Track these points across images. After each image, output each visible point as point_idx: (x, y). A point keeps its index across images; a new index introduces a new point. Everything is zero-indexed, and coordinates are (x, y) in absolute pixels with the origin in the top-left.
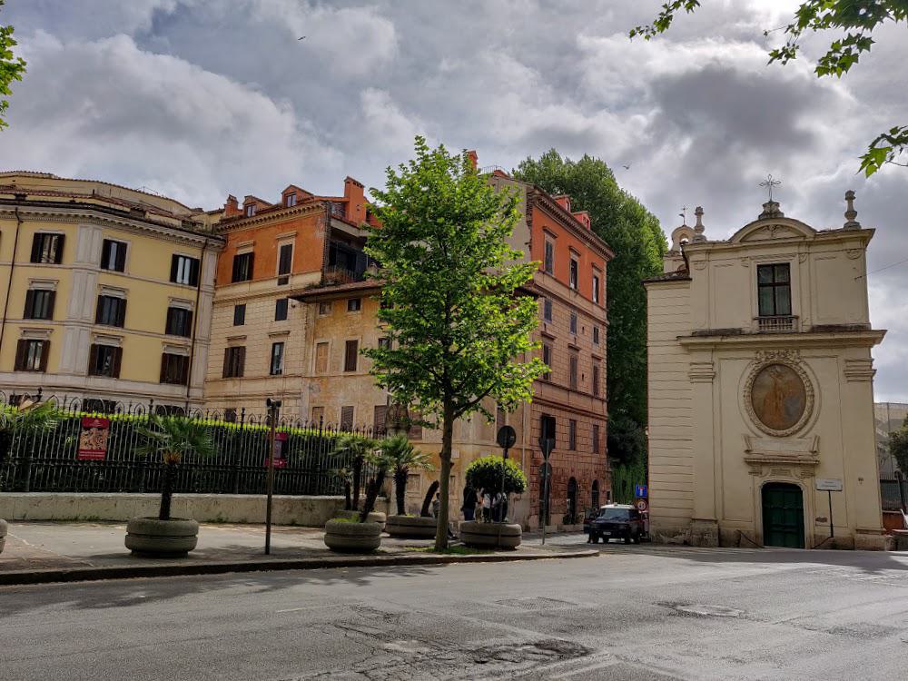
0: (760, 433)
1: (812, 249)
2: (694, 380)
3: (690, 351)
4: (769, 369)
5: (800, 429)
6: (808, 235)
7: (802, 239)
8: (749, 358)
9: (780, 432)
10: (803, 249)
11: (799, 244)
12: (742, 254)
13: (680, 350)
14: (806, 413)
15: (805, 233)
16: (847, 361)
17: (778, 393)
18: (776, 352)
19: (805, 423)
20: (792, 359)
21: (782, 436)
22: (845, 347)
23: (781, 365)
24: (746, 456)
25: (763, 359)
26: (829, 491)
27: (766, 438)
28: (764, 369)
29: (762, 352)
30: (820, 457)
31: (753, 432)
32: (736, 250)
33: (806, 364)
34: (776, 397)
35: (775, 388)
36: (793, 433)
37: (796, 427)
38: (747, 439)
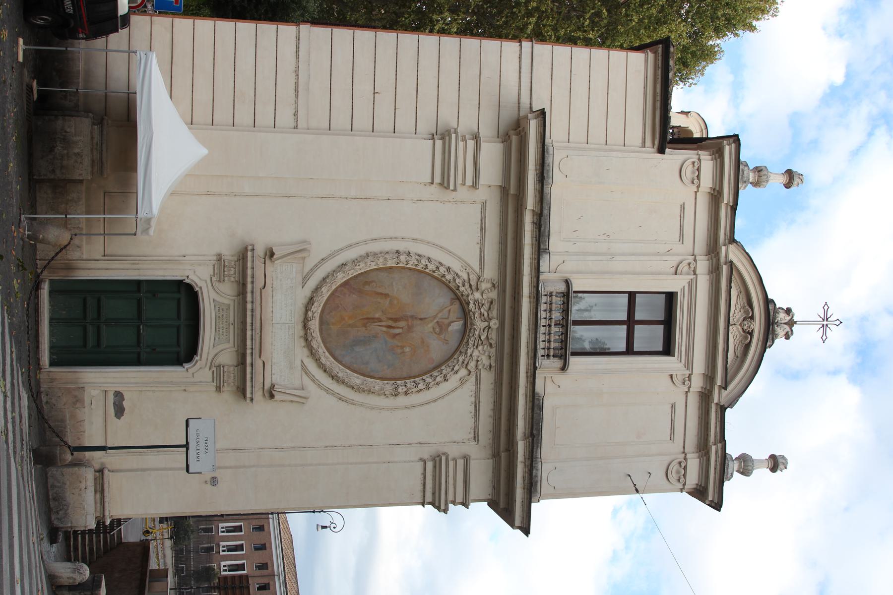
0: (312, 283)
1: (693, 401)
2: (439, 143)
3: (505, 138)
4: (456, 306)
6: (724, 393)
7: (719, 381)
8: (482, 268)
9: (314, 325)
10: (697, 383)
11: (710, 377)
12: (703, 265)
13: (508, 115)
14: (357, 379)
15: (730, 388)
16: (467, 459)
17: (402, 324)
18: (494, 324)
20: (476, 353)
21: (305, 326)
22: (496, 455)
24: (260, 251)
25: (477, 295)
26: (187, 446)
27: (302, 295)
30: (261, 406)
31: (313, 270)
32: (713, 250)
33: (462, 381)
34: (396, 320)
35: (413, 317)
36: (313, 353)
37: (327, 359)
38: (300, 251)
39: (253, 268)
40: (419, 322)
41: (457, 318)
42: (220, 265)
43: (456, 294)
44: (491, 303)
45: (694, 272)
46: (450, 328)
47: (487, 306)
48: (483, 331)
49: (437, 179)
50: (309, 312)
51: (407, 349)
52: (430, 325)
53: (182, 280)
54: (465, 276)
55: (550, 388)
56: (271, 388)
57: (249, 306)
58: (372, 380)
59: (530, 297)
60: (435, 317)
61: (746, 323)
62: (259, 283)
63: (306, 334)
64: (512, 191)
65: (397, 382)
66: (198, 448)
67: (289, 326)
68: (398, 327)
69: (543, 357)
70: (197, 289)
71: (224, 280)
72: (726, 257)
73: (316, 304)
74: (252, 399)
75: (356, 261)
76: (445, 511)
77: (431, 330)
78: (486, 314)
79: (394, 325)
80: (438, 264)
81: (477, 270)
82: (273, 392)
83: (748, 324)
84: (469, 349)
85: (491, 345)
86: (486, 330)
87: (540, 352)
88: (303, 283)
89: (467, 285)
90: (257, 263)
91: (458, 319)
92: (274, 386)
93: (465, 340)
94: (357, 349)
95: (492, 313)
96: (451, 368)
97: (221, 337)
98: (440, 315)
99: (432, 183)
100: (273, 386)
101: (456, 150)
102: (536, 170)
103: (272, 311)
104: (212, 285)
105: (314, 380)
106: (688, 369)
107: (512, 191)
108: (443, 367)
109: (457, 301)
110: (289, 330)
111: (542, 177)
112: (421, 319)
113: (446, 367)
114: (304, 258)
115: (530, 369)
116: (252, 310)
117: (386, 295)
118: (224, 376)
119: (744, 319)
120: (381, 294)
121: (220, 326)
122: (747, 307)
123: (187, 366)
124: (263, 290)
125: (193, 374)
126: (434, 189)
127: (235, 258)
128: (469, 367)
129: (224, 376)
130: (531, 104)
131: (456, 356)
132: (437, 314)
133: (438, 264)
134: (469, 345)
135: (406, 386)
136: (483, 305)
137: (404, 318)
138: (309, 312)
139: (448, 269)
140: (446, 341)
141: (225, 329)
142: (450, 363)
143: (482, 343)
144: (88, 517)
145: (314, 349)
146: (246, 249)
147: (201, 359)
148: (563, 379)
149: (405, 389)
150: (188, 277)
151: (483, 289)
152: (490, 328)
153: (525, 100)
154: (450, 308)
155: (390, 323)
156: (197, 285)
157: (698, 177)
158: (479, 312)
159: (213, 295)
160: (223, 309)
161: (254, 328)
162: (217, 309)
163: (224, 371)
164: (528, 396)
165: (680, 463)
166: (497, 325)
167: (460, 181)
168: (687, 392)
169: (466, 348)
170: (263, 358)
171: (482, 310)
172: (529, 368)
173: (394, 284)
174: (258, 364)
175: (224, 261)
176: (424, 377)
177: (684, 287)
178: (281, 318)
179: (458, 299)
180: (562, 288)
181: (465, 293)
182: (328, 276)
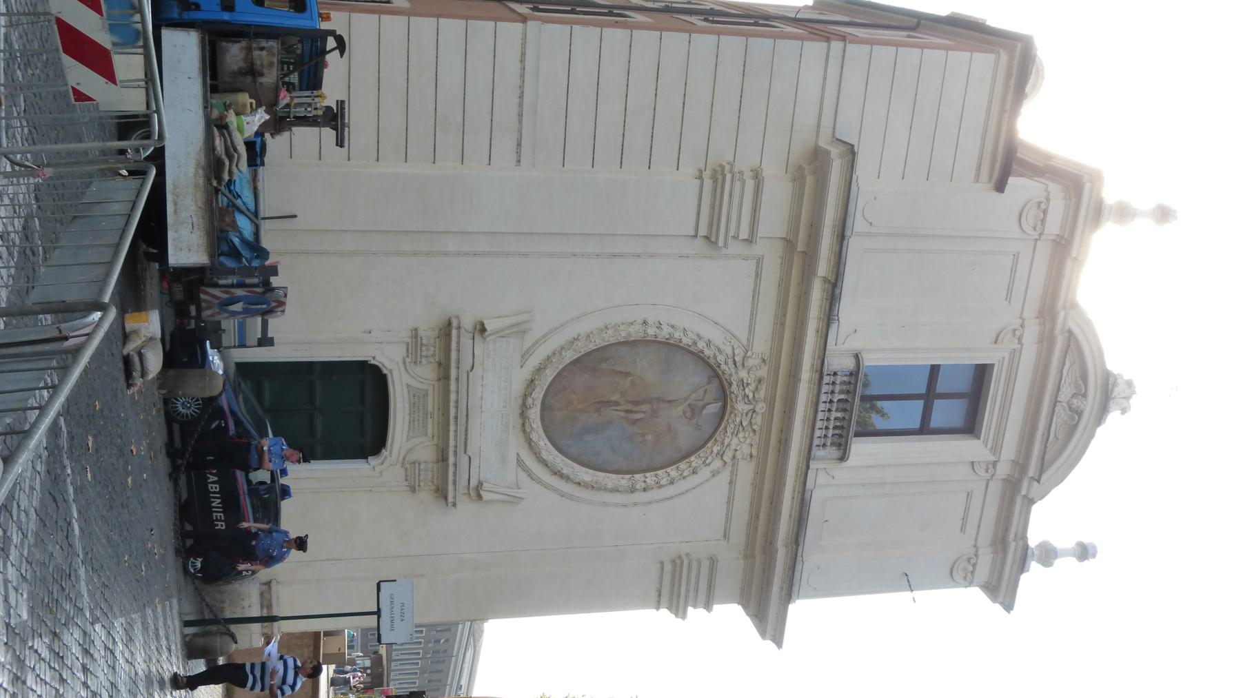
0: (534, 362)
1: (996, 487)
2: (708, 183)
3: (798, 177)
5: (545, 463)
7: (1032, 471)
10: (1003, 470)
12: (1031, 333)
14: (585, 474)
16: (713, 561)
17: (645, 407)
18: (761, 407)
19: (558, 473)
20: (735, 441)
22: (749, 555)
23: (721, 415)
24: (468, 322)
25: (743, 374)
26: (378, 613)
27: (519, 378)
28: (714, 373)
29: (763, 372)
30: (466, 508)
33: (715, 474)
34: (636, 403)
35: (659, 400)
38: (519, 330)
39: (458, 351)
40: (666, 405)
41: (714, 400)
42: (416, 342)
43: (714, 371)
44: (760, 381)
45: (1019, 340)
46: (705, 412)
47: (753, 386)
48: (746, 415)
49: (703, 231)
50: (529, 399)
51: (649, 437)
52: (680, 409)
53: (367, 361)
54: (729, 350)
55: (822, 479)
57: (453, 397)
58: (604, 474)
59: (810, 382)
60: (686, 399)
61: (1075, 401)
62: (466, 365)
63: (523, 424)
64: (800, 247)
65: (635, 475)
66: (392, 616)
68: (639, 412)
69: (818, 448)
70: (385, 371)
71: (420, 362)
72: (1064, 324)
73: (538, 389)
74: (454, 505)
75: (591, 335)
76: (684, 617)
77: (681, 413)
78: (751, 395)
79: (635, 409)
80: (695, 338)
81: (745, 342)
82: (481, 492)
83: (1078, 403)
84: (726, 438)
85: (754, 431)
86: (750, 415)
87: (816, 442)
88: (522, 361)
89: (730, 362)
90: (463, 339)
91: (716, 400)
92: (482, 484)
93: (723, 425)
95: (759, 393)
96: (703, 459)
98: (693, 396)
99: (696, 236)
100: (480, 484)
101: (731, 195)
102: (834, 226)
103: (483, 377)
104: (405, 367)
105: (531, 475)
106: (994, 455)
107: (800, 247)
108: (692, 458)
109: (716, 379)
110: (502, 418)
111: (841, 236)
112: (669, 402)
113: (696, 457)
115: (802, 468)
116: (457, 402)
117: (627, 374)
118: (419, 475)
119: (1074, 396)
120: (621, 372)
122: (1080, 382)
123: (373, 461)
124: (470, 373)
125: (381, 472)
126: (699, 244)
127: (436, 333)
128: (724, 458)
129: (419, 475)
130: (834, 128)
131: (709, 445)
132: (690, 395)
133: (695, 338)
134: (727, 432)
135: (645, 481)
136: (748, 384)
137: (649, 401)
138: (529, 399)
139: (709, 343)
140: (698, 427)
141: (421, 419)
142: (701, 453)
143: (744, 429)
144: (253, 636)
145: (533, 442)
146: (450, 324)
147: (391, 453)
148: (842, 472)
149: (644, 485)
150: (374, 358)
151: (750, 366)
152: (754, 411)
153: (827, 121)
154: (706, 387)
155: (630, 407)
157: (1043, 221)
158: (743, 394)
159: (407, 379)
160: (419, 396)
161: (458, 423)
162: (412, 395)
163: (419, 479)
164: (796, 492)
165: (969, 559)
166: (764, 410)
167: (732, 233)
168: (988, 480)
169: (723, 436)
170: (469, 453)
171: (747, 391)
172: (800, 465)
173: (638, 360)
174: (463, 459)
175: (421, 338)
176: (669, 470)
177: (1004, 358)
179: (717, 376)
180: (850, 364)
181: (728, 372)
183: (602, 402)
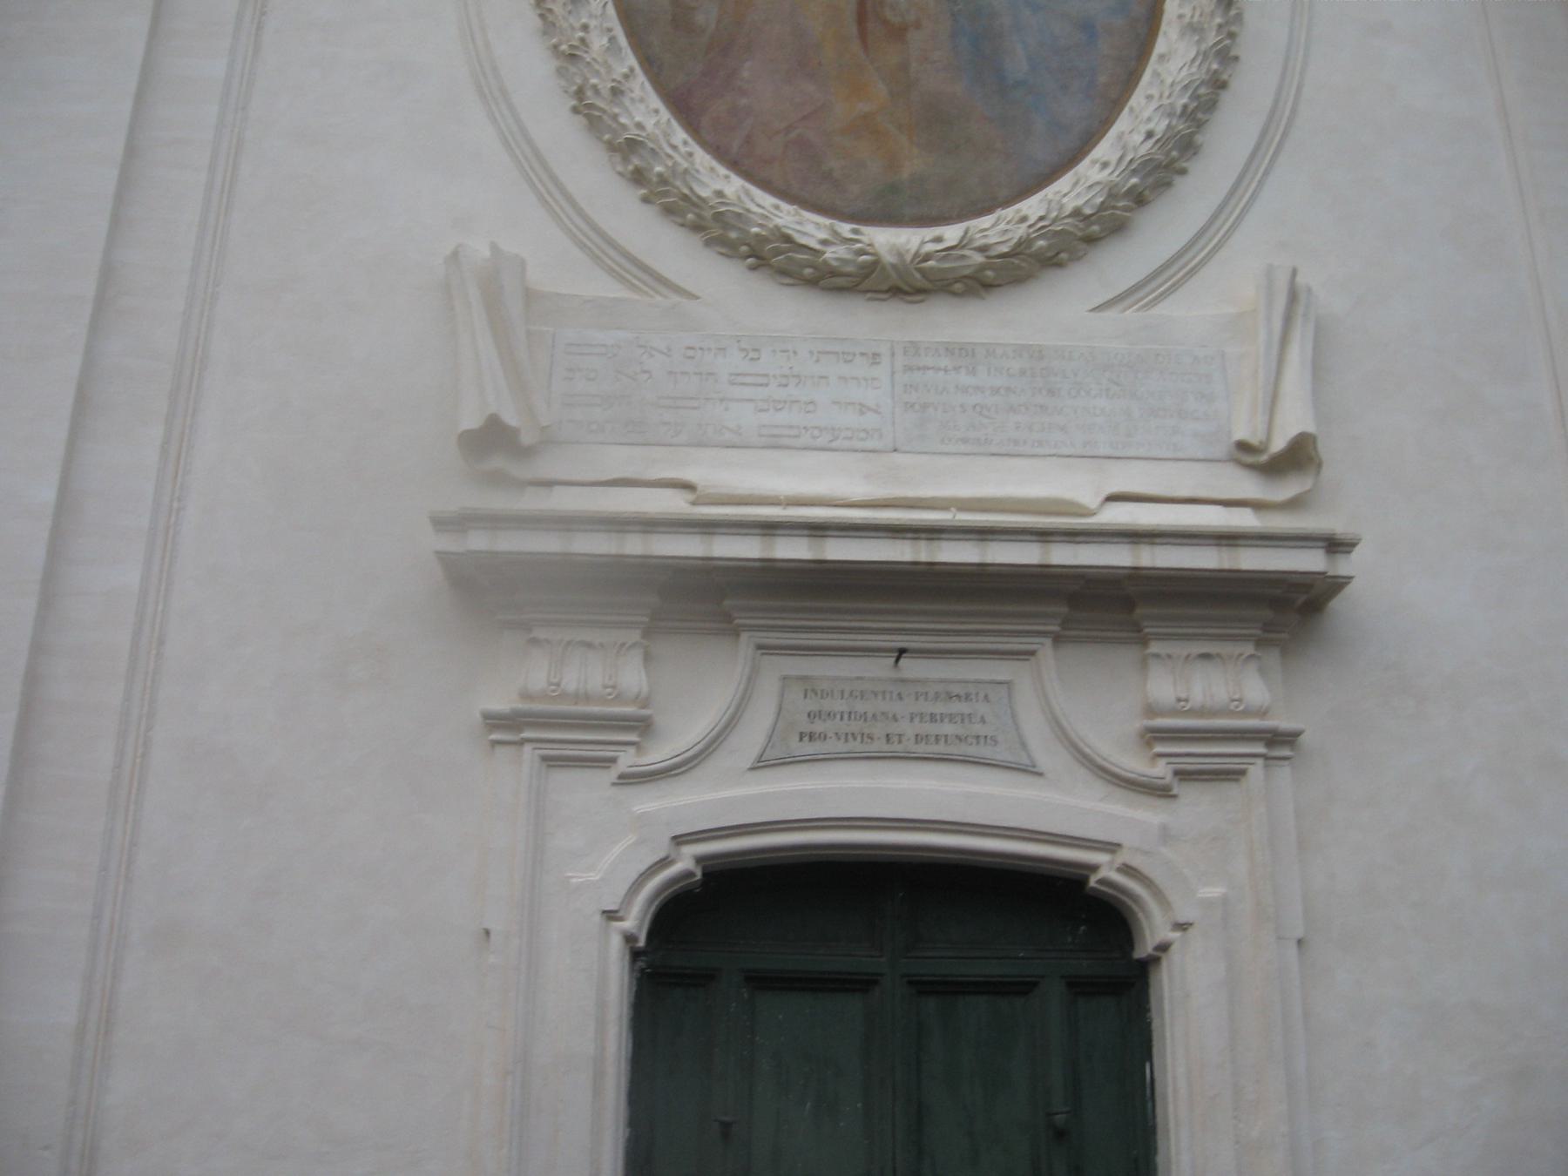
56: (1251, 467)
62: (673, 503)
67: (909, 369)
70: (685, 862)
82: (1278, 444)
92: (1243, 446)
94: (1017, 63)
97: (978, 729)
110: (926, 368)
114: (530, 296)
121: (909, 729)
123: (1154, 929)
150: (611, 915)
156: (664, 863)
162: (809, 748)
178: (863, 409)
182: (638, 177)
183: (861, 18)
